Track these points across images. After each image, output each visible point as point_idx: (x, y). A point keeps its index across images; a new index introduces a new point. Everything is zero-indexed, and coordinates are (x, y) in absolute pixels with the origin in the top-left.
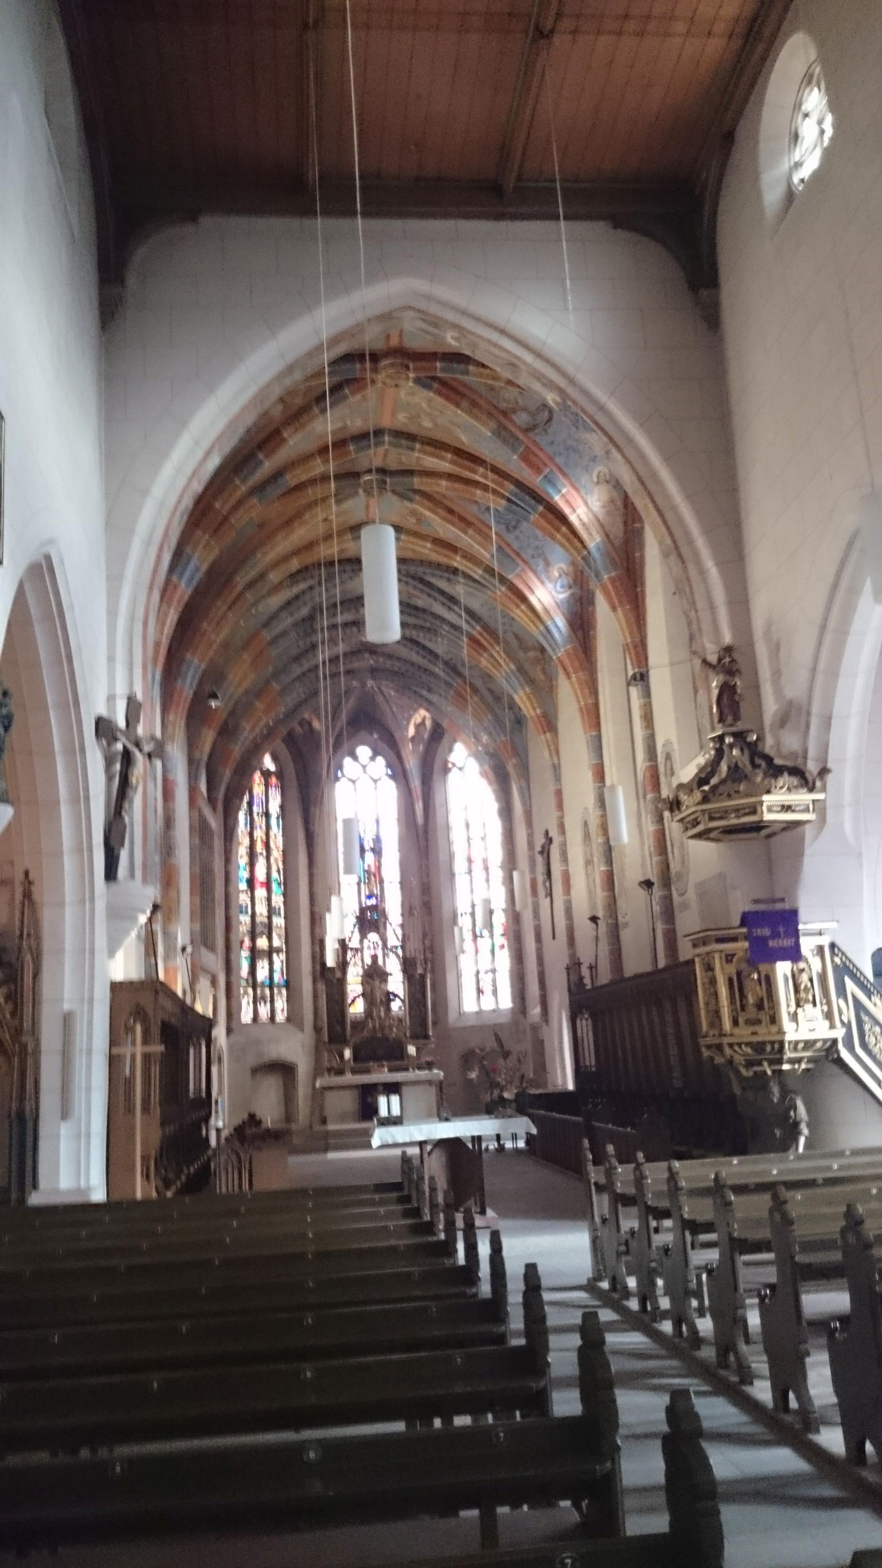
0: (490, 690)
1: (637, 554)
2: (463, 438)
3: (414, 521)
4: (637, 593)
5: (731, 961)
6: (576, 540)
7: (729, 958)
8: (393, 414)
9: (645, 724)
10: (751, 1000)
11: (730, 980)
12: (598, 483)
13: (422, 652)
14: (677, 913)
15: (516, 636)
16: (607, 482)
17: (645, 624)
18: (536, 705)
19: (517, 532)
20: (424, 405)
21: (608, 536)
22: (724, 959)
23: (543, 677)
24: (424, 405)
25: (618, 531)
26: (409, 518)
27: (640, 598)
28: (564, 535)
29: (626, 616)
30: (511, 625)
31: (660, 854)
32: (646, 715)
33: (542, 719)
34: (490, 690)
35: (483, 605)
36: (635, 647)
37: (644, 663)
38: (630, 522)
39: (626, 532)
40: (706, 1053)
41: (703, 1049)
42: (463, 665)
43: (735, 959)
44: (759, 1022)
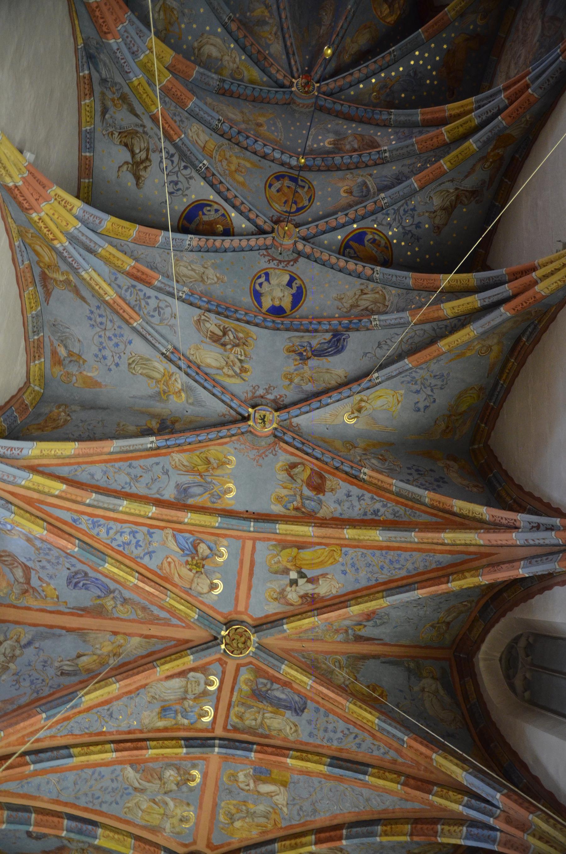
0: (137, 115)
2: (130, 772)
3: (203, 549)
8: (205, 776)
13: (222, 189)
15: (83, 299)
18: (41, 224)
19: (73, 569)
20: (171, 804)
23: (38, 248)
24: (171, 804)
26: (208, 552)
30: (92, 312)
33: (26, 205)
34: (137, 115)
35: (130, 342)
42: (170, 157)
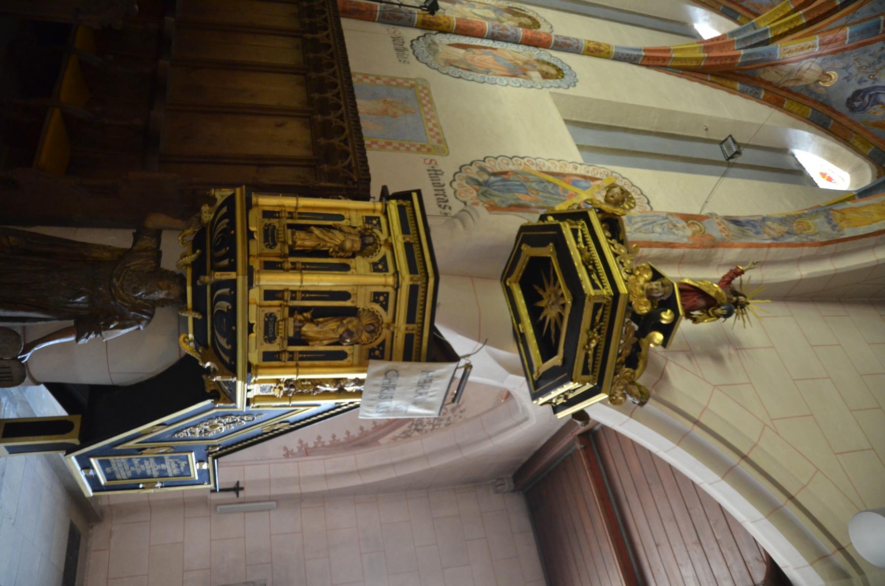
1: (738, 86)
4: (706, 74)
5: (376, 301)
6: (786, 29)
7: (382, 298)
9: (592, 46)
10: (309, 329)
11: (344, 295)
12: (824, 73)
14: (391, 29)
16: (818, 81)
17: (681, 76)
21: (772, 65)
22: (381, 289)
25: (770, 75)
27: (702, 76)
28: (798, 19)
29: (697, 59)
31: (458, 27)
32: (601, 51)
36: (664, 59)
37: (646, 63)
38: (769, 88)
39: (762, 81)
40: (221, 195)
41: (228, 192)
43: (377, 307)
44: (270, 338)
